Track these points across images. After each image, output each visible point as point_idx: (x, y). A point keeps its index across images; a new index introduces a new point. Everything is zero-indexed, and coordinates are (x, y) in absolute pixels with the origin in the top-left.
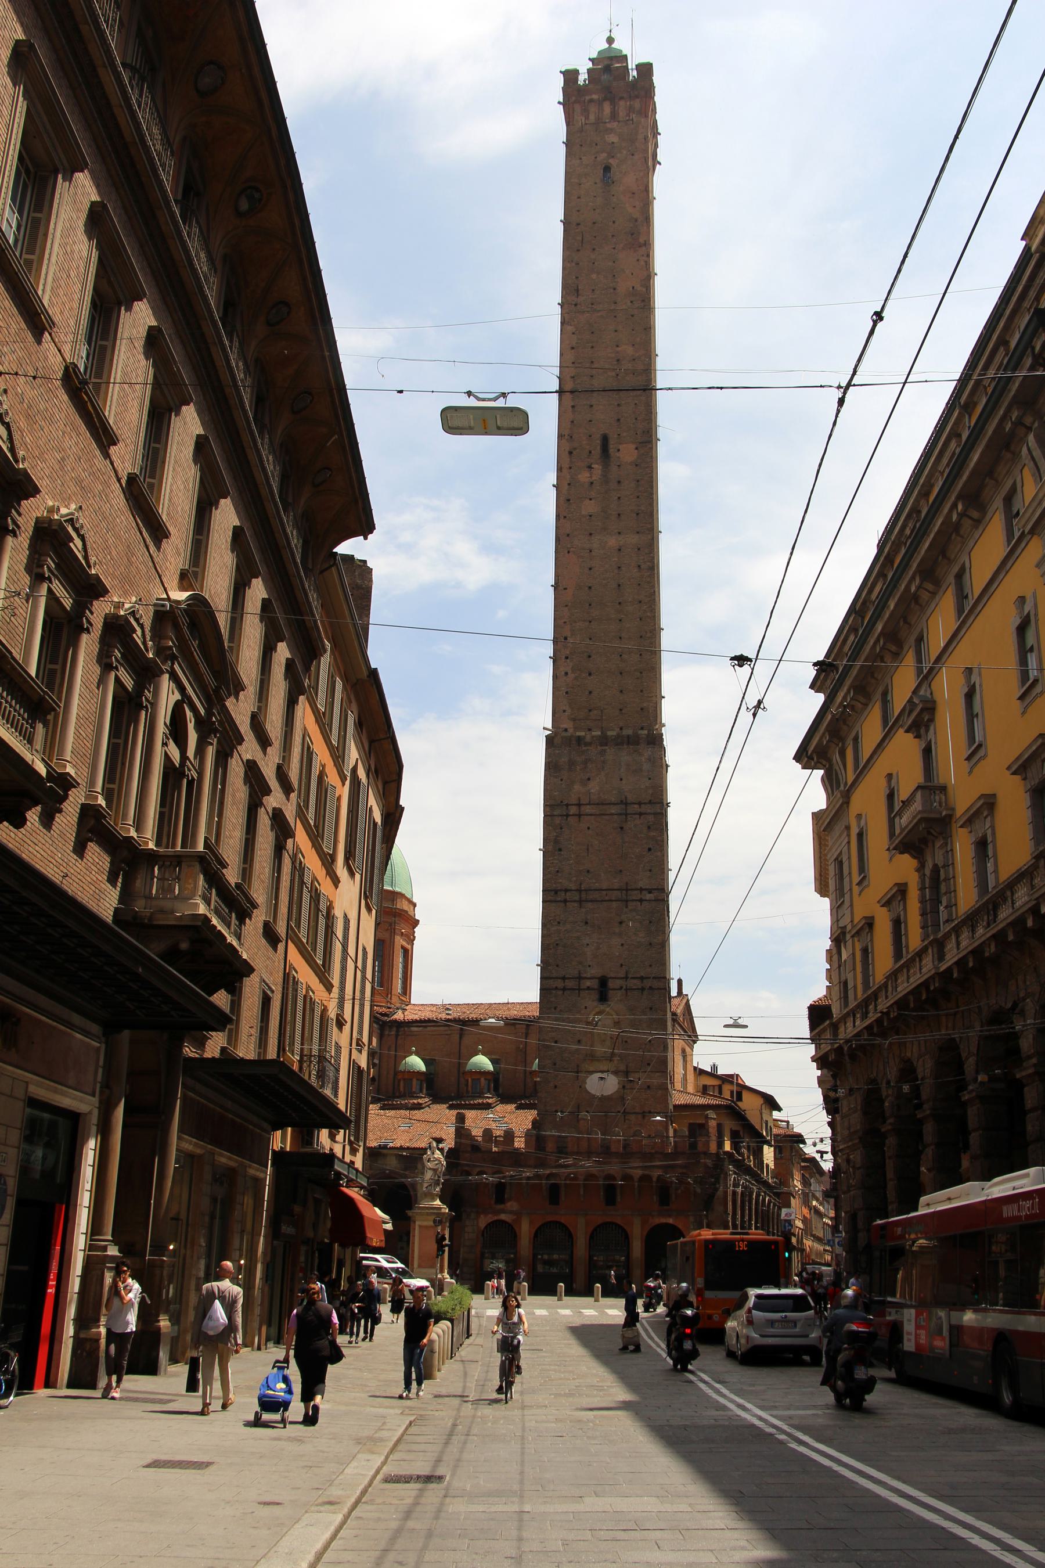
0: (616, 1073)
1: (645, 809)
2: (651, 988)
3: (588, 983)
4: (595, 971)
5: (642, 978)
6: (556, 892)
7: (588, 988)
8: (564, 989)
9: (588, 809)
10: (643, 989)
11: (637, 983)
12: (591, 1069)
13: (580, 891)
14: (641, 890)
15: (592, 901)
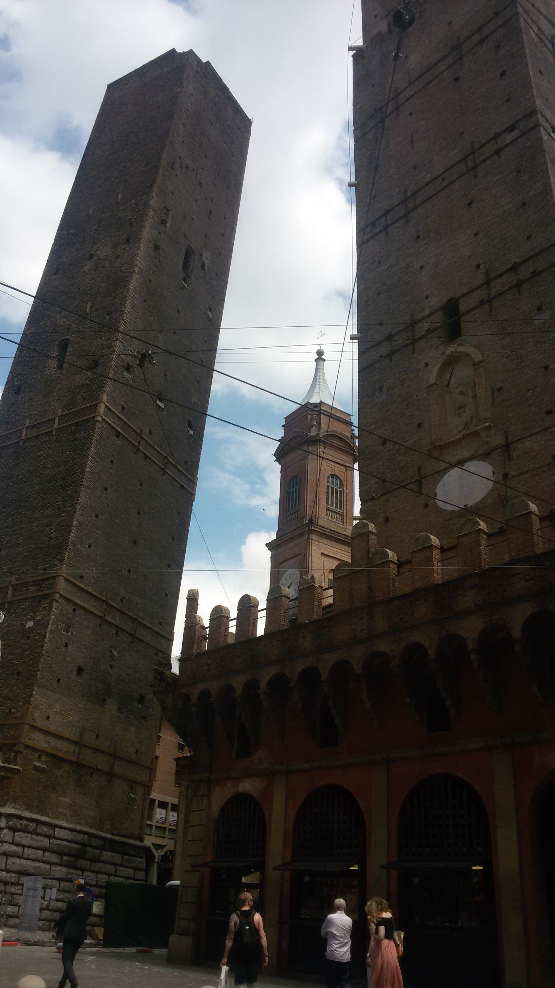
0: (486, 456)
2: (536, 274)
4: (438, 299)
5: (515, 268)
6: (373, 224)
8: (391, 354)
9: (408, 93)
10: (519, 284)
11: (510, 279)
12: (443, 466)
13: (405, 200)
14: (496, 137)
15: (422, 203)
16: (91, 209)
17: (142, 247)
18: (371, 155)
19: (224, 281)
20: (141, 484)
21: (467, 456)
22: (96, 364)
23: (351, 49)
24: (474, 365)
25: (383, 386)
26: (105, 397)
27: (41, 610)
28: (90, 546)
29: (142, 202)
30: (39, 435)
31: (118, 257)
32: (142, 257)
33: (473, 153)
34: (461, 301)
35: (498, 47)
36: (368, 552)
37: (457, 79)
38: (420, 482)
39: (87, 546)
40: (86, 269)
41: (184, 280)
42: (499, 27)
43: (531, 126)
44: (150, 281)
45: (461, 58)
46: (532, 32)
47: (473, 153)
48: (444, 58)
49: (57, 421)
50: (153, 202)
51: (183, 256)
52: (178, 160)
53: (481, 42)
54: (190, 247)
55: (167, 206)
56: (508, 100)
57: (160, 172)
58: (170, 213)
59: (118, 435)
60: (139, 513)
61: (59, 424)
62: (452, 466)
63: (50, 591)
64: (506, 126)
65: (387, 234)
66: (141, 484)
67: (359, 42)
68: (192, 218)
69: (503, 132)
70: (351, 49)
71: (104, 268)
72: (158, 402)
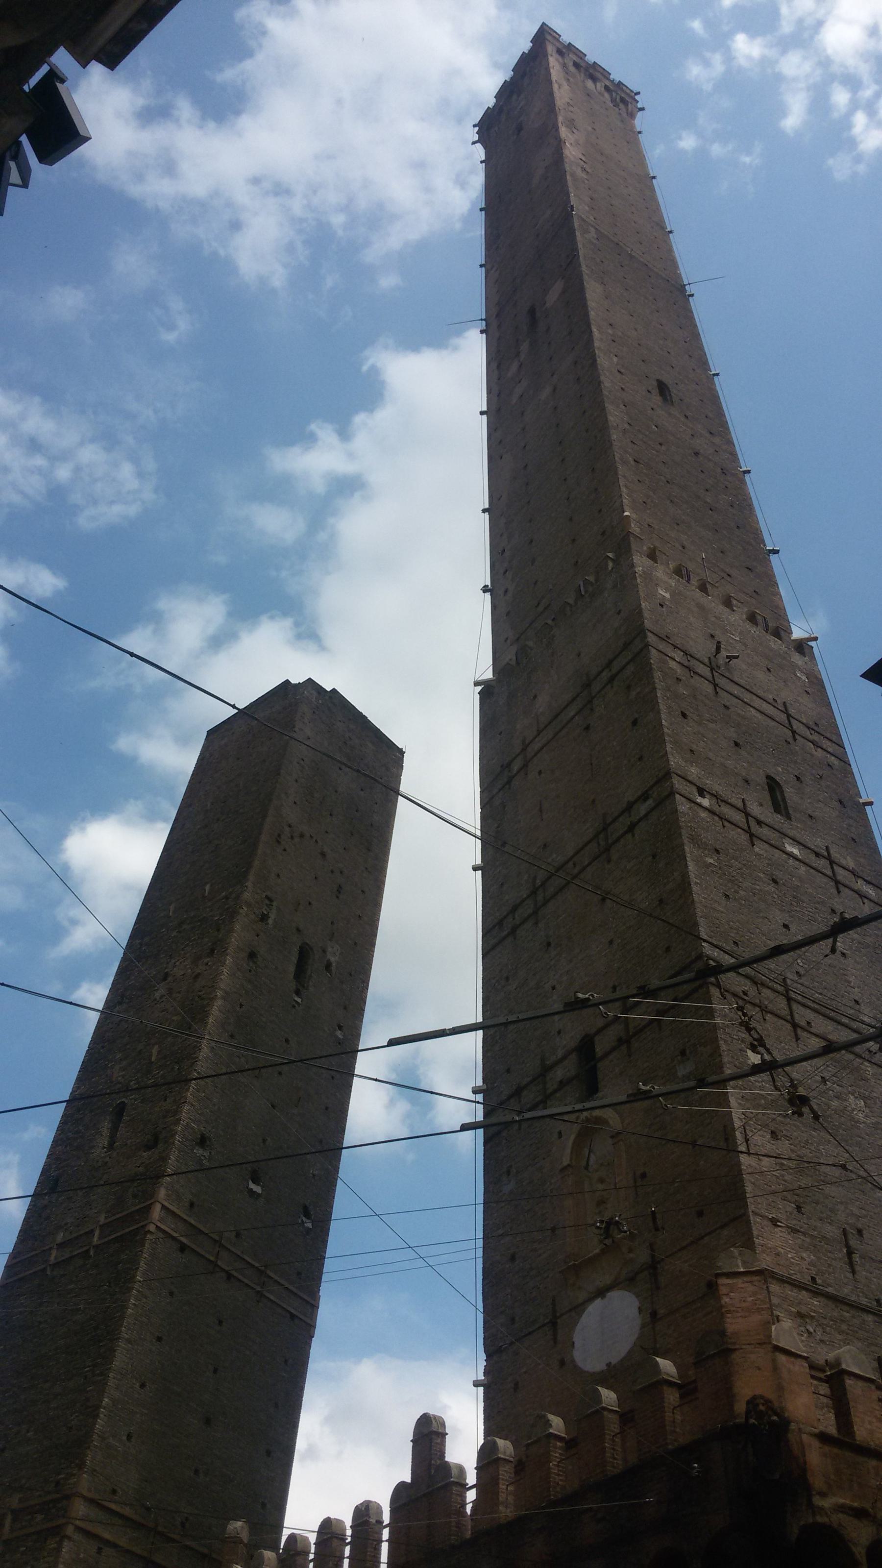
0: (629, 1282)
1: (616, 666)
3: (559, 1073)
6: (500, 923)
7: (562, 1084)
9: (536, 746)
13: (534, 893)
14: (630, 806)
16: (172, 908)
17: (229, 960)
18: (498, 827)
19: (363, 982)
20: (220, 1323)
21: (608, 1282)
22: (153, 1143)
23: (476, 684)
24: (612, 1137)
25: (511, 1166)
26: (162, 1193)
27: (46, 1554)
28: (129, 1437)
29: (234, 895)
30: (74, 1256)
31: (197, 976)
32: (227, 974)
33: (605, 829)
34: (597, 1038)
35: (629, 687)
36: (430, 1465)
37: (587, 728)
38: (554, 1324)
39: (125, 1438)
40: (157, 995)
41: (298, 993)
42: (628, 663)
43: (666, 793)
44: (241, 1006)
45: (590, 702)
46: (672, 664)
47: (605, 829)
48: (574, 699)
49: (97, 1233)
50: (247, 895)
51: (294, 960)
52: (287, 829)
53: (611, 680)
54: (307, 944)
55: (268, 893)
56: (640, 759)
57: (259, 852)
58: (275, 903)
59: (183, 1248)
60: (215, 1371)
61: (100, 1238)
62: (591, 1300)
63: (62, 1521)
64: (640, 793)
65: (515, 938)
66: (220, 1323)
67: (489, 675)
68: (310, 903)
69: (636, 801)
70: (476, 684)
71: (179, 992)
72: (252, 1186)
